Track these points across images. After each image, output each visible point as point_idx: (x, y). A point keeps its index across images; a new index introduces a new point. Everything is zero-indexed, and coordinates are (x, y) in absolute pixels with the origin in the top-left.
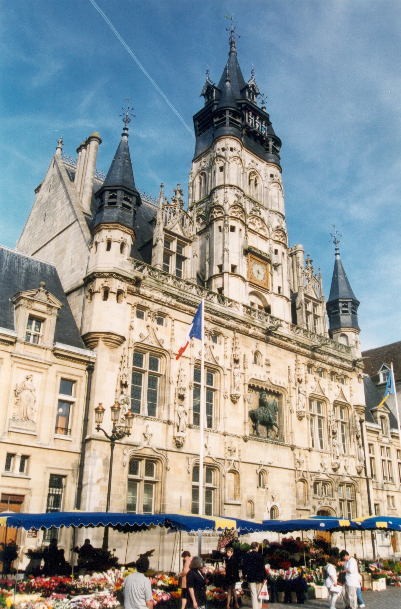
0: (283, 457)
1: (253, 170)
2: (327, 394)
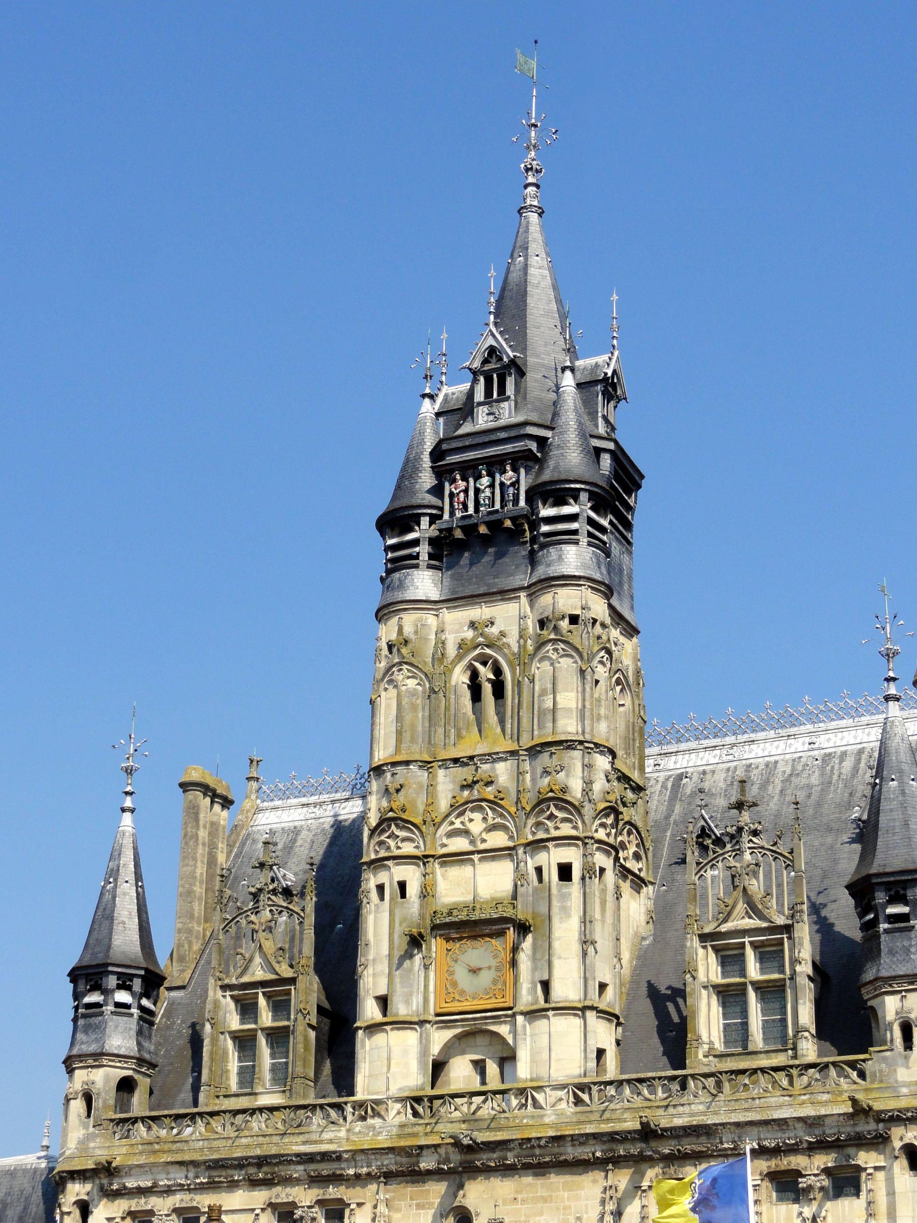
1: (477, 652)
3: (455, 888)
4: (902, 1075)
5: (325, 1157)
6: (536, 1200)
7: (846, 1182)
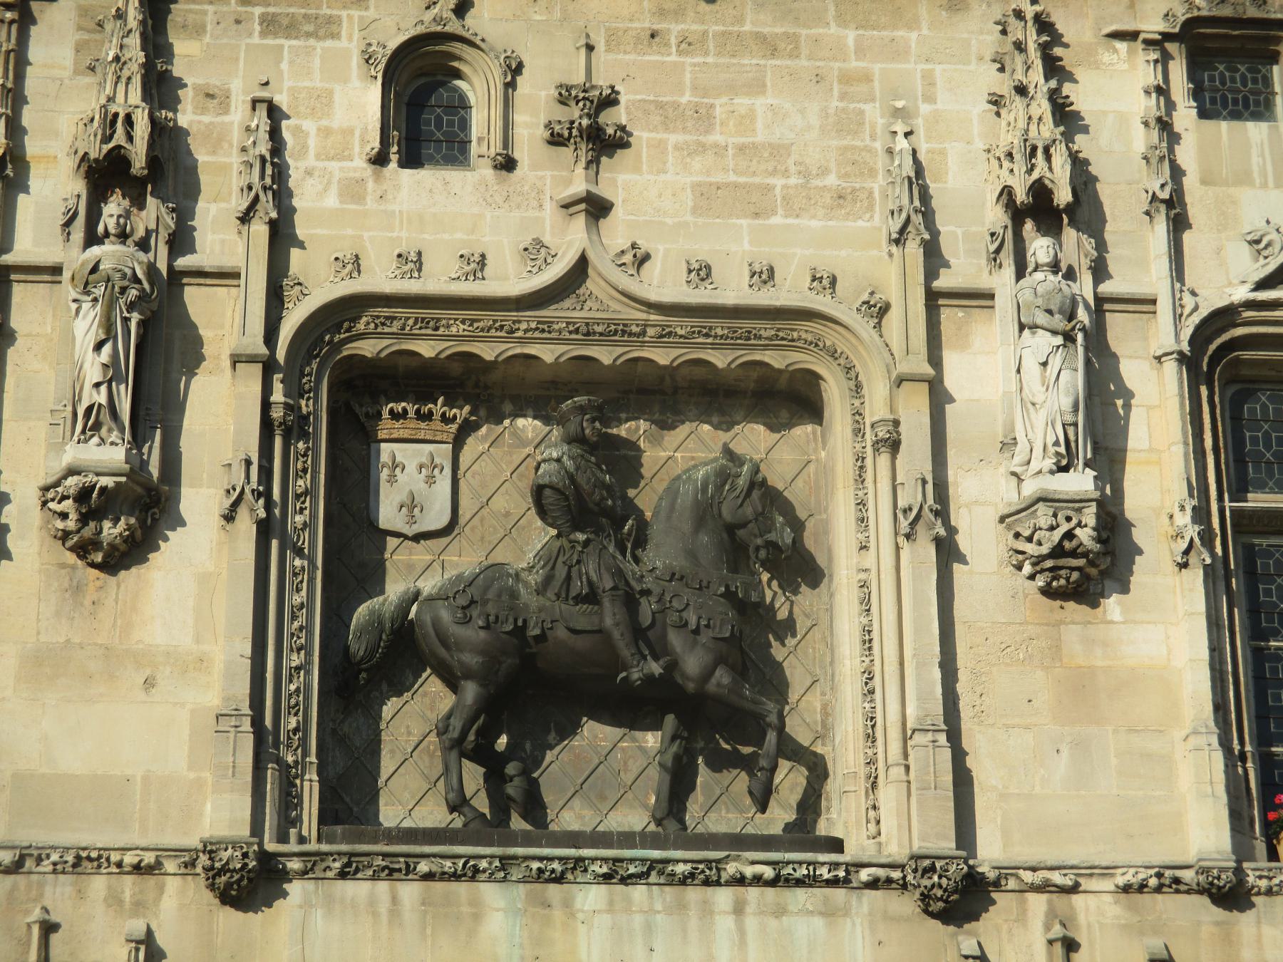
6: (732, 43)
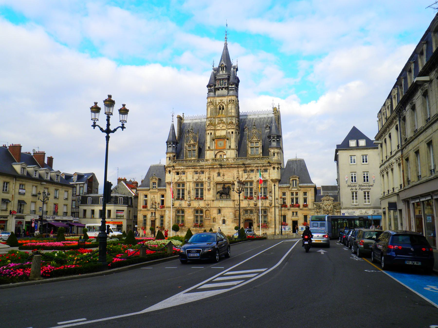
0: (230, 203)
2: (254, 179)
3: (218, 133)
4: (273, 159)
5: (202, 166)
7: (266, 170)
